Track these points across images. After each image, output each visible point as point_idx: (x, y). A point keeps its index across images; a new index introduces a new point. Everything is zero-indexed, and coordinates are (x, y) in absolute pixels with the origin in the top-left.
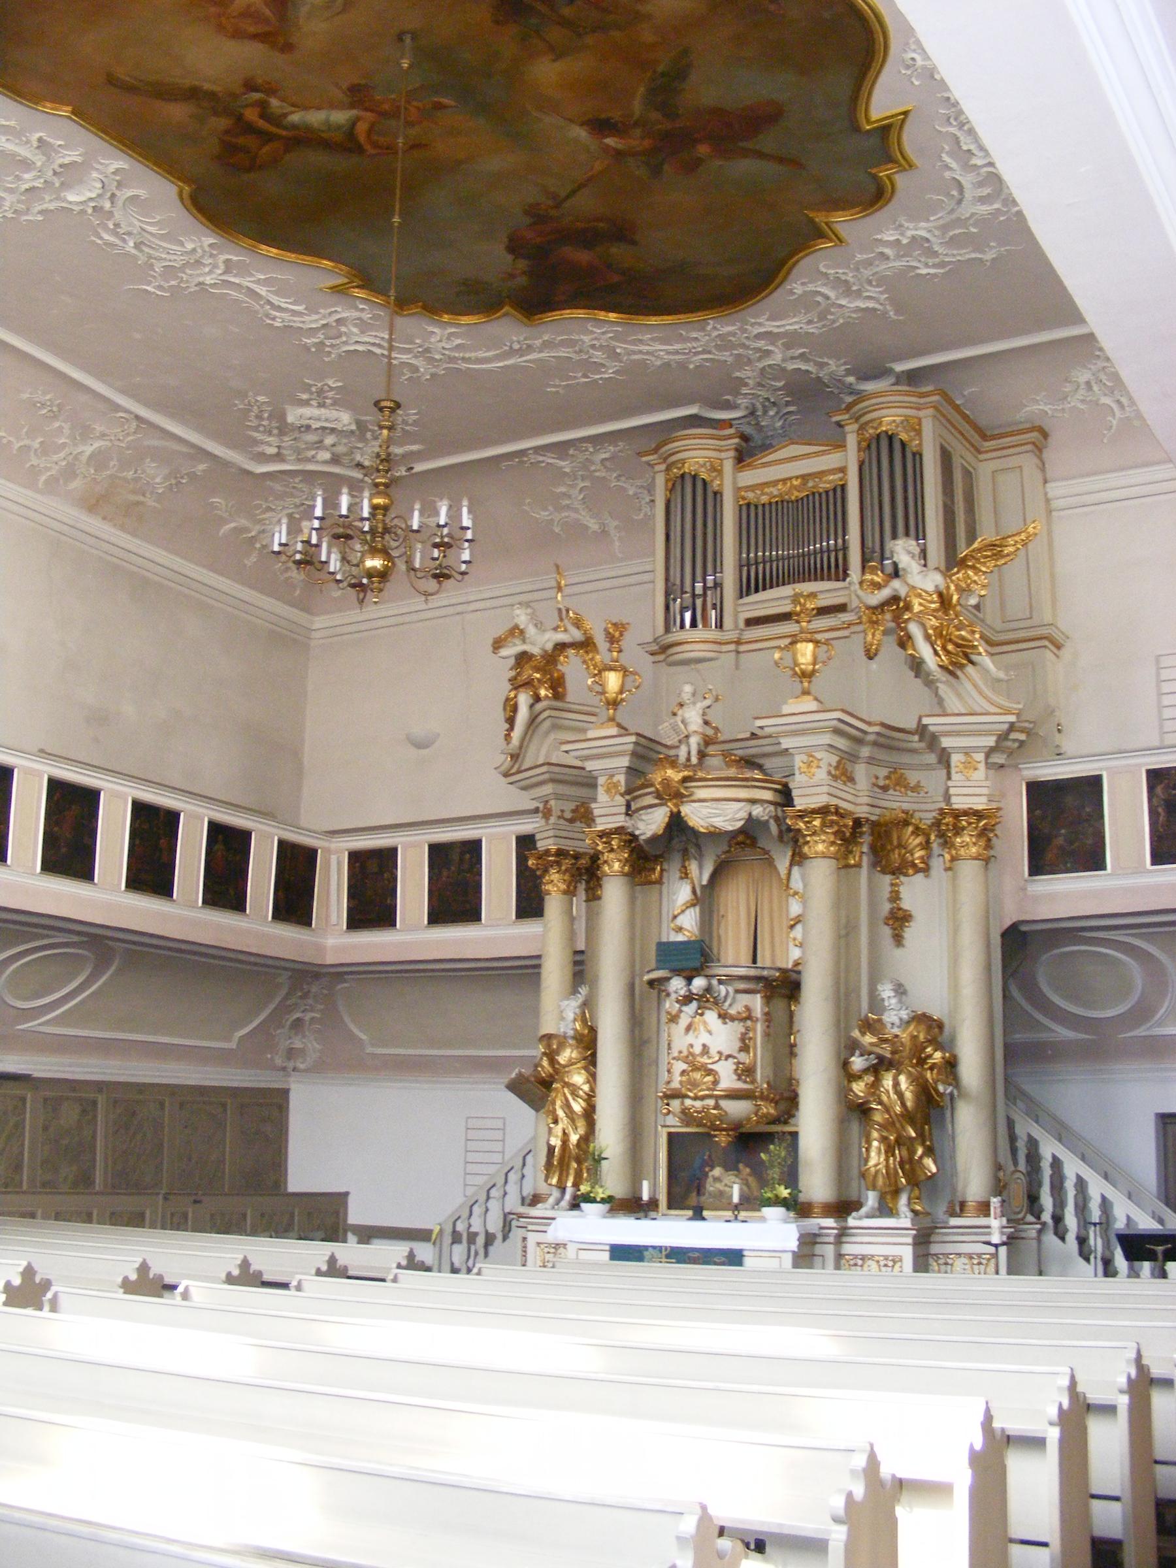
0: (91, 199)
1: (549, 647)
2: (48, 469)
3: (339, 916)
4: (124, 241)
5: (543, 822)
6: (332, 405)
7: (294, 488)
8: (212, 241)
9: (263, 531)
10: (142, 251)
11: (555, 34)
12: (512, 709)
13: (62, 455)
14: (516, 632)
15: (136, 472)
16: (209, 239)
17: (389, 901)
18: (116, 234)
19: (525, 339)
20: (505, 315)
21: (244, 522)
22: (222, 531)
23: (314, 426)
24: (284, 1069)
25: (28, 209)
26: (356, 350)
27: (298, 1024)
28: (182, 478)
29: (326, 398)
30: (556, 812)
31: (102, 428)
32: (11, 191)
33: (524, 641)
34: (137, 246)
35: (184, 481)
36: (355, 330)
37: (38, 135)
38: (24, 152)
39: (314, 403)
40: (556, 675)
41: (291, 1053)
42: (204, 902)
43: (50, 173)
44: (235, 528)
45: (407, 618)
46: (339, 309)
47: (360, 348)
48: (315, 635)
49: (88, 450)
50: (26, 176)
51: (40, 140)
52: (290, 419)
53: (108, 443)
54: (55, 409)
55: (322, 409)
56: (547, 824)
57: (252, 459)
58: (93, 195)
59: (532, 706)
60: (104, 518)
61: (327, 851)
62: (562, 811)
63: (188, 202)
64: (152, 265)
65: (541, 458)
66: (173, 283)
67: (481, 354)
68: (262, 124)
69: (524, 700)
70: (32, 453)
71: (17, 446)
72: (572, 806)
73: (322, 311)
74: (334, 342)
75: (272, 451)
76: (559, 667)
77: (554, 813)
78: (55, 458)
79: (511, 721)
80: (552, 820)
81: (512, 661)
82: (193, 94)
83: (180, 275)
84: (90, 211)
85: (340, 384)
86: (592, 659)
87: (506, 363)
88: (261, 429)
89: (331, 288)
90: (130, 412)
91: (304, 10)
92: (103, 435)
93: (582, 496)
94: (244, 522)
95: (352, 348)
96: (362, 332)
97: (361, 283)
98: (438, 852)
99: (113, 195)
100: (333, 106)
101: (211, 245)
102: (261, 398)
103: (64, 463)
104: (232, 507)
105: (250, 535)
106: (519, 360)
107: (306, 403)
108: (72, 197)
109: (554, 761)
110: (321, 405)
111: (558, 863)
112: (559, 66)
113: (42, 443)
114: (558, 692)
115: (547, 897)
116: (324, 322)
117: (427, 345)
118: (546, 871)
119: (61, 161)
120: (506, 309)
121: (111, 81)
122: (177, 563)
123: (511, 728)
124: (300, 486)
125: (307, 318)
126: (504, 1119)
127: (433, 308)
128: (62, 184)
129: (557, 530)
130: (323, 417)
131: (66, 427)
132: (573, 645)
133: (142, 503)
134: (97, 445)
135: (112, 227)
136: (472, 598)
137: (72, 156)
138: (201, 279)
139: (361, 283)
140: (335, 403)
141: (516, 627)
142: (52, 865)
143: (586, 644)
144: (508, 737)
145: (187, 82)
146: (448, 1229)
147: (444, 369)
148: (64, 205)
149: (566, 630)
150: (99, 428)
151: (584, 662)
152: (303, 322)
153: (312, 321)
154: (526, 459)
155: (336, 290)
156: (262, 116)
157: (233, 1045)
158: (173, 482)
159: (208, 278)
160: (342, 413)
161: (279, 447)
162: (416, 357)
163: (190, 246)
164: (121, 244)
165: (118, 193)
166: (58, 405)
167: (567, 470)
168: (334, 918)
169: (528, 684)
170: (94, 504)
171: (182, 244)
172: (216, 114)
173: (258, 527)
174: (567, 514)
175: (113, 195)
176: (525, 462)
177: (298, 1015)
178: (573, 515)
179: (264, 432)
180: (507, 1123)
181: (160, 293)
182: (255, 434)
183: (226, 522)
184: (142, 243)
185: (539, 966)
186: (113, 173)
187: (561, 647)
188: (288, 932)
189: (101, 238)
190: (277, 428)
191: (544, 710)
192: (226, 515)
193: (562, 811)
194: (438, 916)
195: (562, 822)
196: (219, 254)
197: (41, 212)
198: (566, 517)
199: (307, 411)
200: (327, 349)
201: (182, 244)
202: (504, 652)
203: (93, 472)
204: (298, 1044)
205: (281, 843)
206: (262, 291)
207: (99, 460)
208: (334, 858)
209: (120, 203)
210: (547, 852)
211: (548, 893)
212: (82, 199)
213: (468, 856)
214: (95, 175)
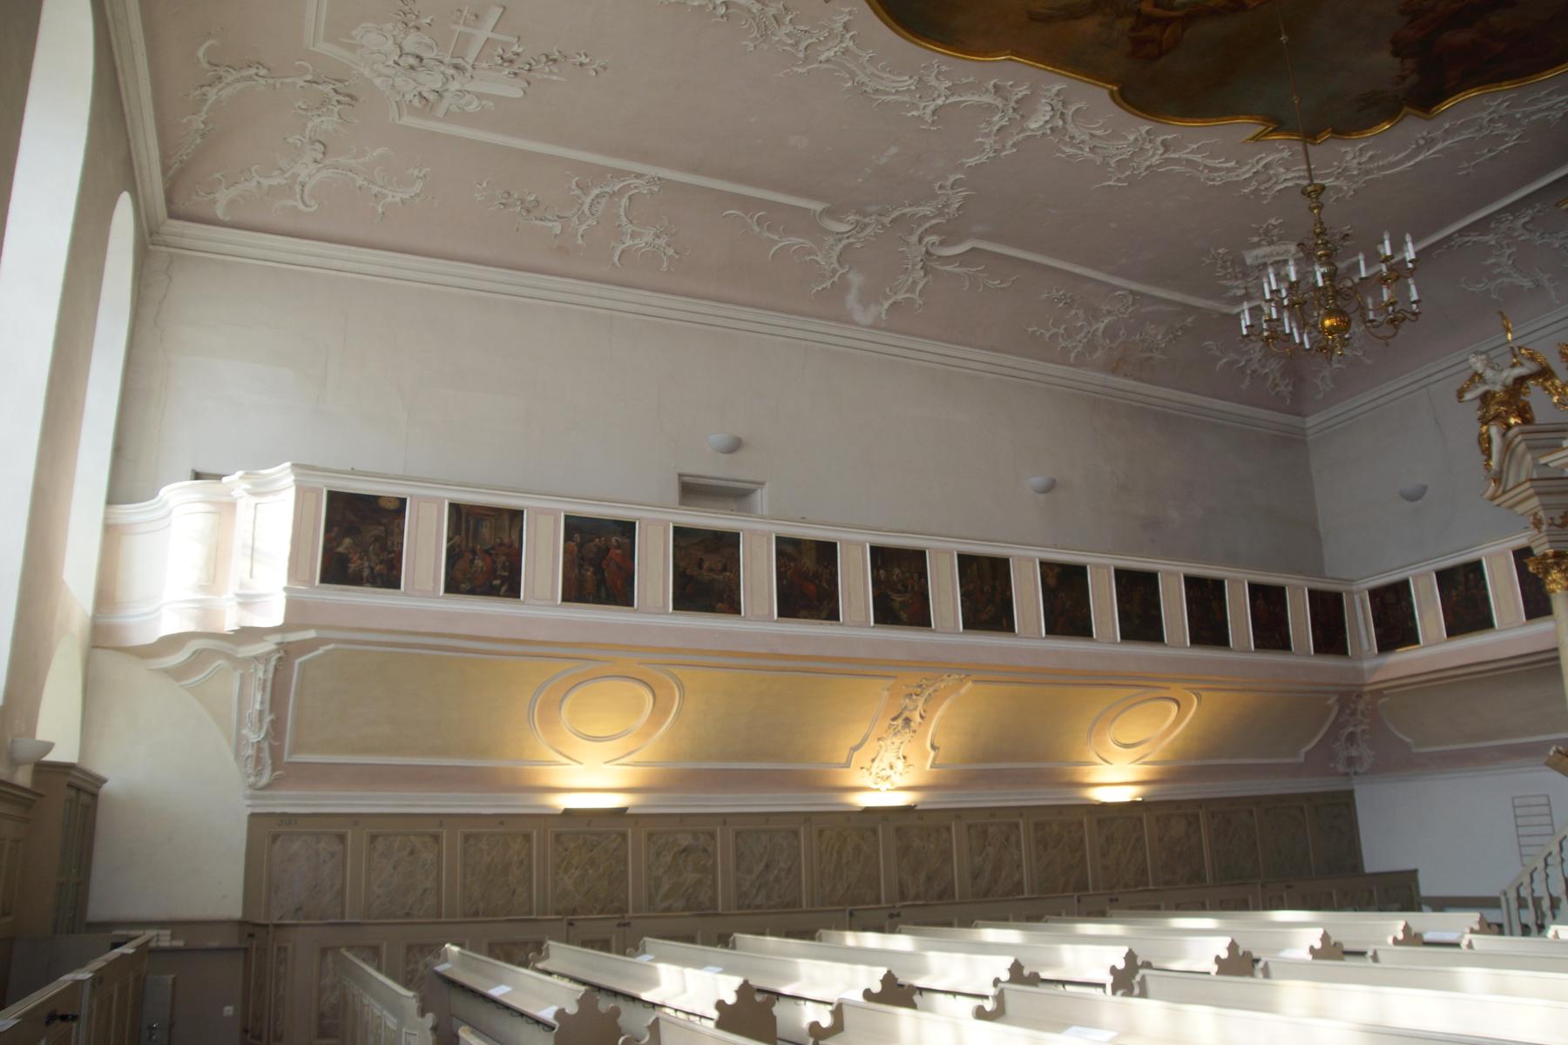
0: (1046, 122)
1: (1509, 381)
2: (1075, 347)
3: (1370, 644)
4: (1082, 149)
5: (1536, 531)
6: (1279, 240)
8: (1147, 128)
9: (1251, 360)
10: (1095, 153)
12: (1485, 443)
13: (1083, 334)
14: (1477, 377)
15: (1141, 335)
16: (1145, 127)
17: (1410, 624)
18: (1073, 146)
19: (1429, 133)
20: (1405, 116)
21: (1233, 356)
22: (1218, 368)
23: (1269, 262)
24: (1347, 774)
25: (1004, 146)
26: (1286, 187)
27: (1351, 738)
28: (1177, 331)
29: (1272, 236)
30: (1545, 520)
31: (1108, 307)
32: (987, 135)
33: (1485, 382)
34: (1092, 149)
36: (1282, 170)
37: (992, 83)
38: (987, 99)
39: (1264, 243)
40: (1521, 405)
41: (1350, 761)
42: (1256, 647)
43: (1011, 111)
46: (1264, 155)
47: (1290, 184)
49: (1102, 326)
51: (995, 86)
52: (1249, 261)
53: (1114, 318)
54: (1069, 301)
55: (1273, 246)
56: (1540, 532)
58: (1047, 118)
59: (1504, 435)
60: (1125, 376)
61: (1351, 593)
62: (1552, 519)
63: (1120, 100)
64: (1108, 163)
65: (1467, 239)
66: (1128, 173)
67: (1393, 159)
69: (1494, 431)
70: (1061, 339)
71: (1048, 335)
72: (1561, 513)
73: (1250, 161)
74: (1267, 185)
75: (1240, 292)
76: (1523, 398)
77: (1545, 522)
78: (1078, 338)
79: (1488, 453)
80: (1544, 528)
81: (1478, 403)
83: (1131, 164)
84: (1049, 132)
85: (1280, 221)
86: (1553, 384)
87: (1418, 159)
88: (1228, 276)
89: (1251, 139)
90: (1124, 289)
92: (1109, 312)
93: (1510, 262)
94: (1233, 356)
95: (1282, 186)
96: (1288, 170)
97: (1276, 126)
98: (1444, 577)
99: (1062, 114)
101: (1147, 132)
102: (1221, 251)
103: (1085, 340)
105: (1240, 365)
106: (1427, 154)
107: (1258, 245)
108: (1033, 126)
109: (1535, 476)
110: (1271, 243)
111: (1558, 564)
113: (1065, 329)
114: (1527, 418)
115: (1553, 595)
116: (1255, 170)
117: (1344, 165)
118: (1547, 572)
119: (1015, 98)
120: (1406, 109)
121: (1033, 17)
122: (1189, 397)
123: (1490, 457)
125: (1240, 171)
126: (1548, 796)
127: (1345, 129)
128: (1022, 116)
129: (1494, 297)
130: (1275, 253)
131: (1081, 312)
132: (1531, 376)
133: (1151, 358)
134: (1106, 321)
135: (1068, 140)
136: (1432, 371)
137: (1022, 91)
138: (1148, 163)
139: (1276, 126)
140: (1281, 238)
141: (1476, 374)
142: (1129, 634)
143: (1545, 373)
144: (1487, 466)
146: (1512, 895)
147: (1364, 183)
148: (1028, 133)
149: (1522, 365)
150: (1105, 307)
151: (1546, 389)
152: (1237, 176)
153: (1246, 172)
154: (1453, 243)
155: (1256, 138)
157: (1301, 759)
158: (1171, 336)
159: (1153, 160)
160: (1289, 246)
161: (1246, 288)
162: (1337, 178)
163: (1131, 138)
164: (1080, 153)
165: (1065, 111)
166: (1070, 297)
167: (1493, 243)
168: (1365, 646)
169: (1496, 417)
170: (1114, 367)
171: (1125, 138)
173: (1245, 357)
174: (1500, 281)
175: (1062, 114)
176: (1452, 246)
177: (1351, 729)
178: (1506, 280)
179: (1231, 279)
180: (1551, 799)
181: (1120, 184)
182: (1225, 282)
184: (1094, 147)
185: (1557, 658)
186: (1057, 95)
187: (1521, 380)
188: (1330, 662)
189: (1064, 152)
190: (1240, 272)
191: (1516, 436)
192: (1218, 353)
193: (1552, 519)
194: (1454, 630)
195: (1554, 528)
196: (1156, 137)
197: (1013, 146)
198: (1501, 283)
199: (1260, 252)
200: (1263, 193)
201: (1125, 138)
202: (1468, 396)
203: (1108, 342)
204: (1354, 752)
205: (1311, 592)
206: (1197, 158)
207: (1110, 332)
208: (1357, 598)
209: (1069, 119)
210: (1545, 556)
211: (1553, 591)
212: (1041, 123)
213: (1471, 576)
214: (1044, 101)
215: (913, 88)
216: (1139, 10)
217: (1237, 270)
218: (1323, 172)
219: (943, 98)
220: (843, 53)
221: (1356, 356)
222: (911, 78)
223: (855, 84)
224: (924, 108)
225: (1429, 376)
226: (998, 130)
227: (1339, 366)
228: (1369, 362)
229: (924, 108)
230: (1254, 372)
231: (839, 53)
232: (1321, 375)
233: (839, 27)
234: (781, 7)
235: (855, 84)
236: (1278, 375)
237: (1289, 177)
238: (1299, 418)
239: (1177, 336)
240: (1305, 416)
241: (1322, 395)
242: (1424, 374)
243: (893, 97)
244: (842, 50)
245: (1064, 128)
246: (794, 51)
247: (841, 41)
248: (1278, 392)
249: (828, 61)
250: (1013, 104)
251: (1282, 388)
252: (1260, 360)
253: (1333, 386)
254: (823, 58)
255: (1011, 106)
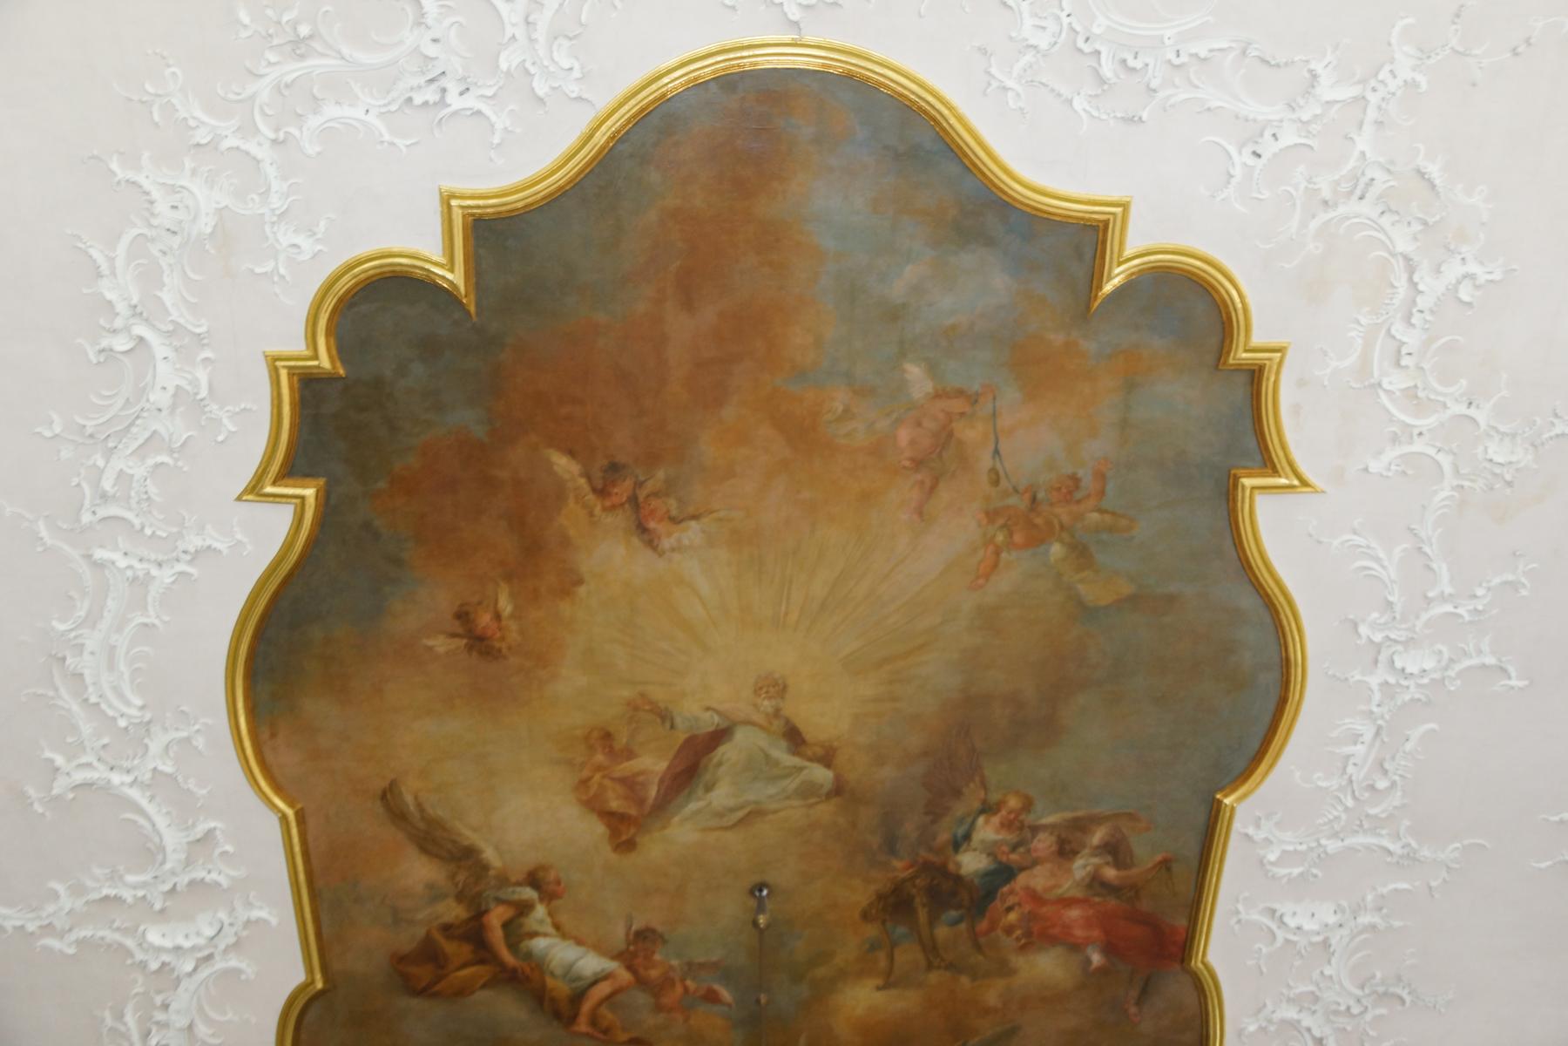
11: (909, 954)
32: (77, 890)
43: (167, 887)
50: (131, 878)
58: (187, 944)
68: (497, 936)
82: (464, 857)
91: (693, 806)
99: (209, 957)
100: (599, 948)
108: (154, 937)
112: (880, 998)
119: (200, 874)
121: (389, 797)
137: (220, 875)
145: (470, 837)
148: (130, 943)
156: (506, 926)
165: (217, 958)
172: (460, 897)
175: (209, 957)
189: (120, 1016)
197: (80, 943)
209: (204, 973)
214: (222, 915)
215: (122, 723)
216: (486, 912)
219: (128, 779)
220: (135, 578)
222: (142, 708)
223: (73, 634)
224: (80, 766)
226: (107, 898)
229: (80, 766)
231: (129, 573)
233: (194, 542)
234: (185, 436)
235: (73, 634)
243: (75, 708)
244: (141, 574)
245: (178, 980)
246: (87, 503)
247: (160, 565)
249: (100, 566)
250: (183, 880)
254: (100, 554)
255: (176, 879)
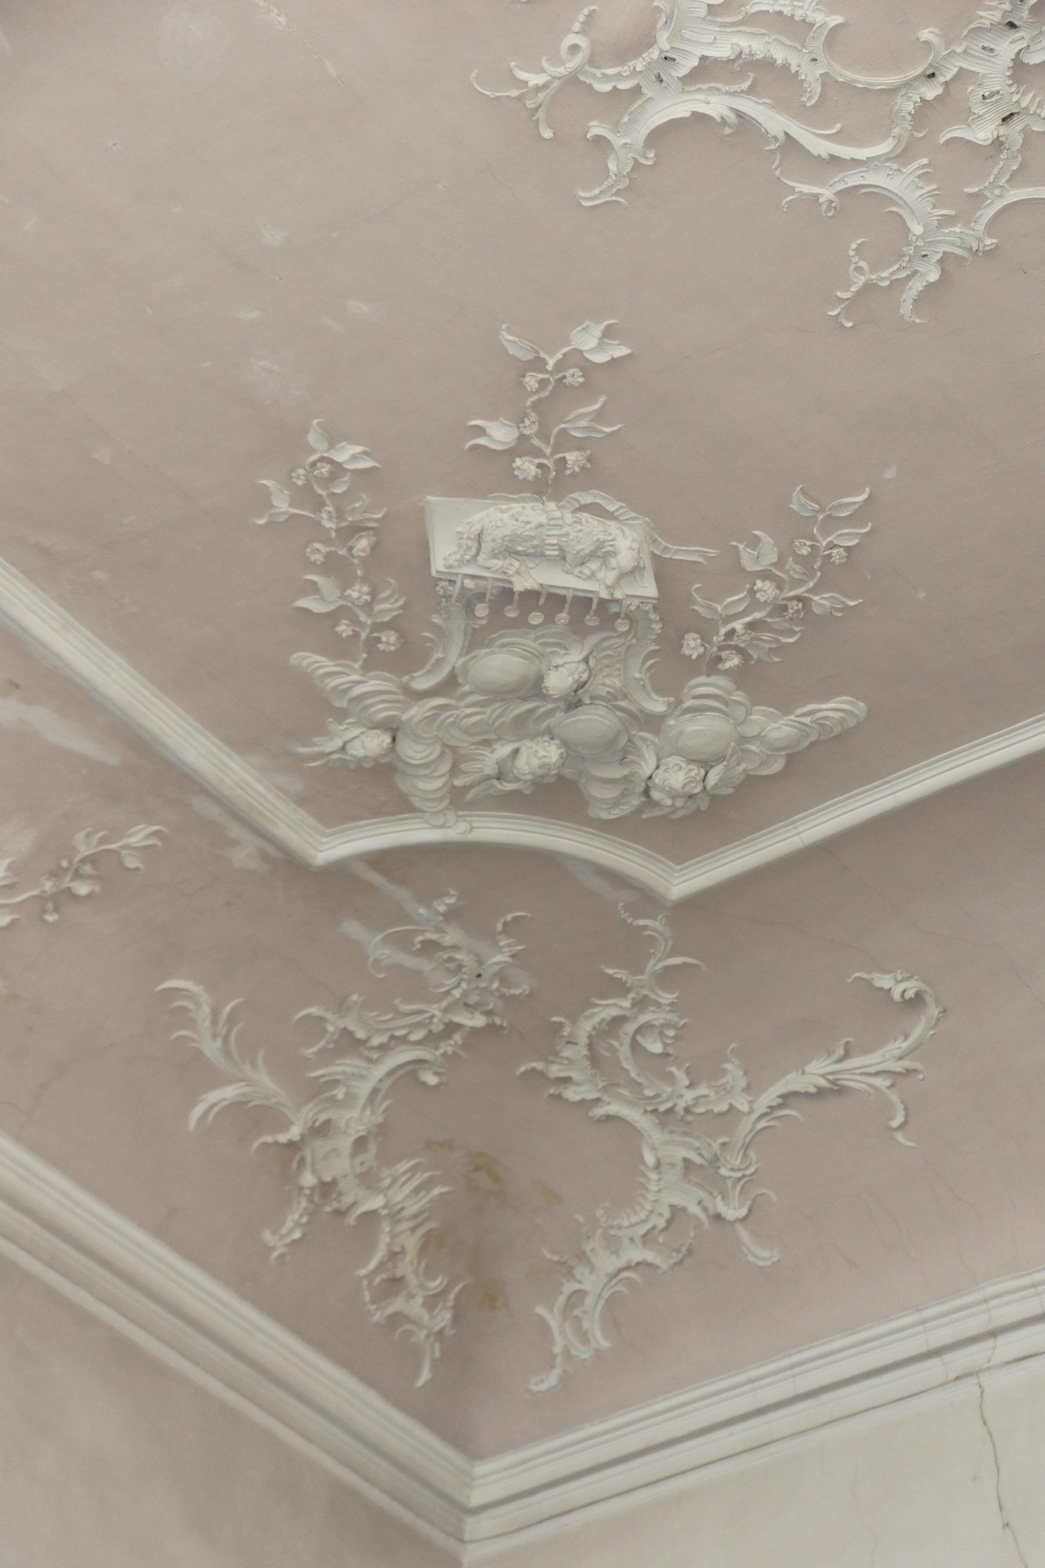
7: (430, 948)
9: (322, 1130)
26: (699, 119)
35: (83, 889)
39: (527, 467)
44: (238, 1106)
45: (782, 1421)
48: (473, 1527)
57: (302, 801)
85: (622, 351)
95: (682, 106)
104: (231, 1020)
105: (282, 1138)
124: (452, 936)
161: (393, 729)
183: (217, 1080)
192: (211, 1049)
200: (596, 129)
217: (388, 608)
218: (862, 79)
221: (718, 1217)
225: (993, 1334)
227: (648, 1255)
228: (763, 1255)
230: (327, 1189)
232: (569, 1287)
236: (412, 1243)
237: (722, 51)
238: (451, 1453)
239: (70, 894)
240: (477, 1456)
241: (552, 1379)
242: (975, 1324)
248: (396, 1319)
251: (415, 1307)
252: (360, 1144)
253: (605, 1344)
